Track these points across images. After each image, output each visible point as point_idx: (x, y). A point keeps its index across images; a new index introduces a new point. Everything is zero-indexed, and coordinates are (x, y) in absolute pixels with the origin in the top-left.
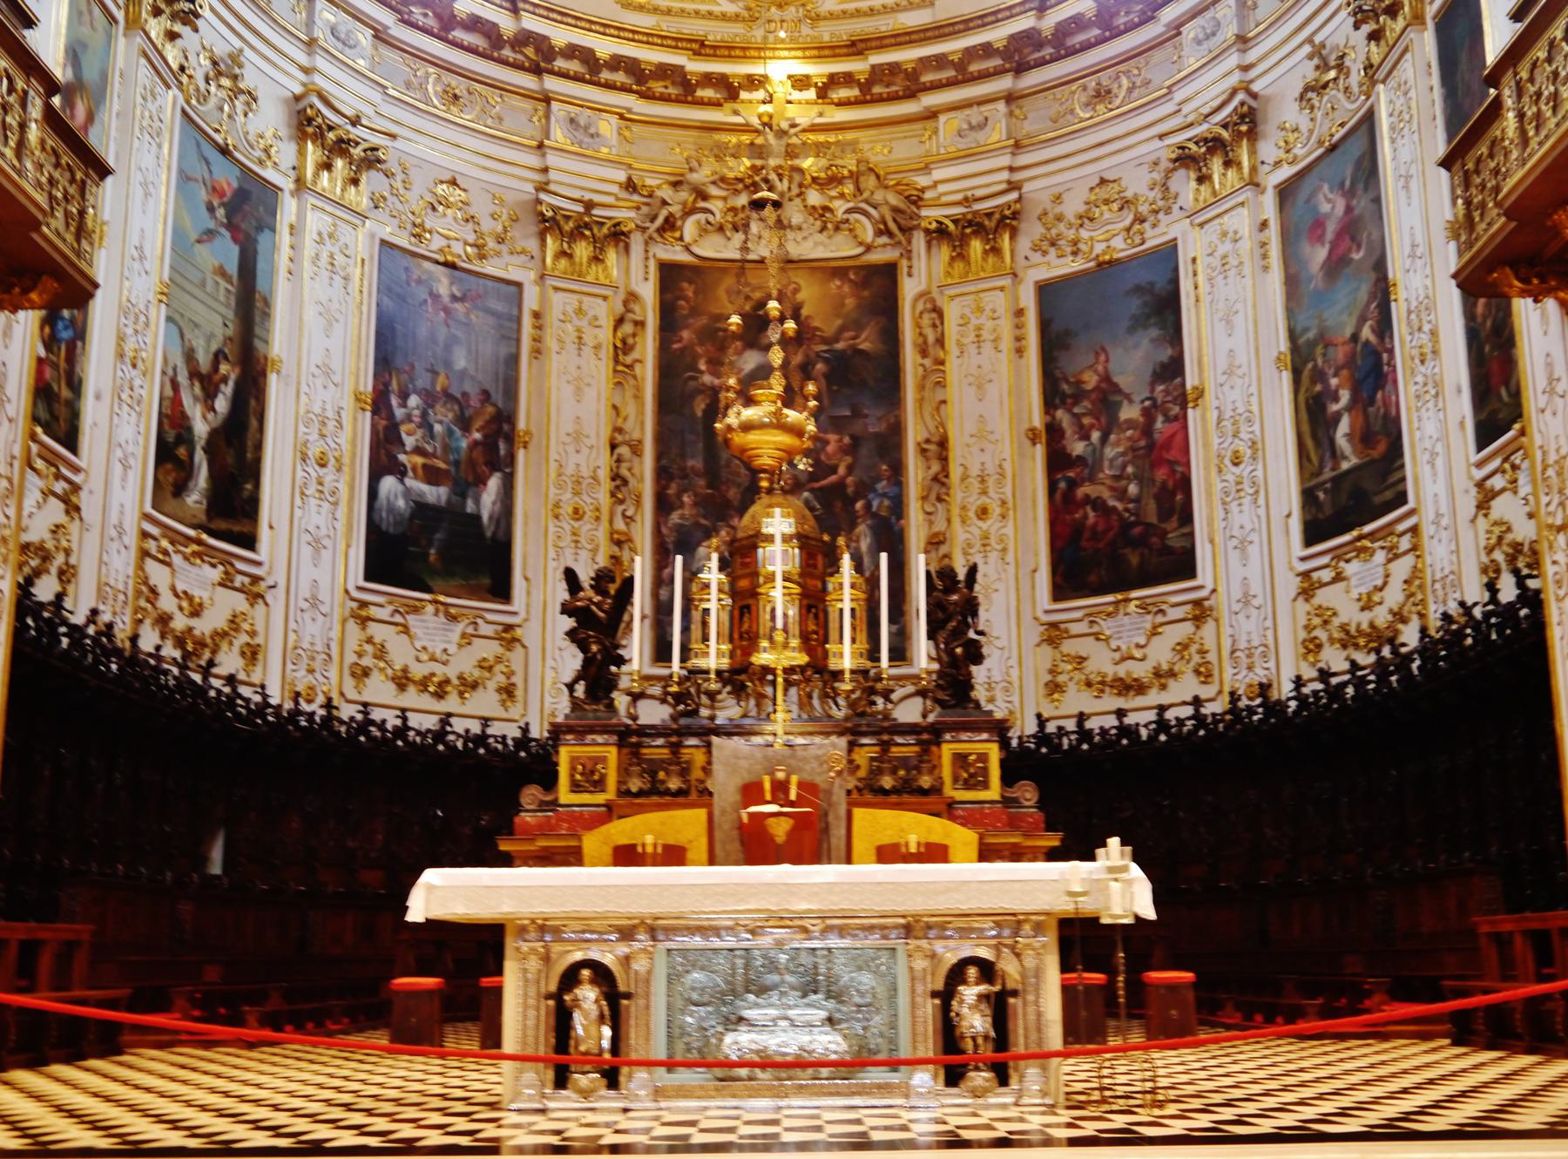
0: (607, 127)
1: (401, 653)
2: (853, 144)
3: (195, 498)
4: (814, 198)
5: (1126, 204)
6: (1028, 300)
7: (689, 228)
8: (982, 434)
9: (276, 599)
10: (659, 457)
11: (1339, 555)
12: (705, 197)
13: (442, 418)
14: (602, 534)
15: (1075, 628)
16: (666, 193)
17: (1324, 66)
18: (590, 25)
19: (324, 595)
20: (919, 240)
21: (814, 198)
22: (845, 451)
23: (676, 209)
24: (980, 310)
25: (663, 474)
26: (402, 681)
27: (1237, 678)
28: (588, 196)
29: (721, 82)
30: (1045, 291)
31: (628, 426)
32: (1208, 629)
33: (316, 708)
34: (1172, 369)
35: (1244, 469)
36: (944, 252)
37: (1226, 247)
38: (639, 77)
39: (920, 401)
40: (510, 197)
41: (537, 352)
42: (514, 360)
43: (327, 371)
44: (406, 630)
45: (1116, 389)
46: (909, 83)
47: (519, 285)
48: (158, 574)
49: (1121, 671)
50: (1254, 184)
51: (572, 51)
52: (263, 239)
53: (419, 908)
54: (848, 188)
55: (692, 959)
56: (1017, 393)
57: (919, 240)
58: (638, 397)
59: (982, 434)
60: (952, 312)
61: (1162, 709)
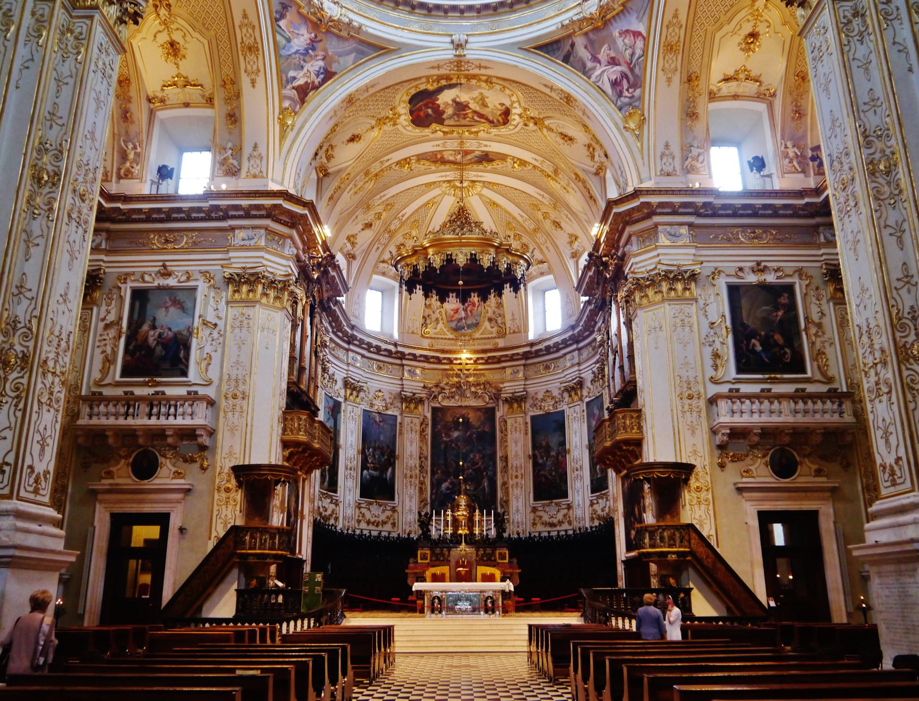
1: (368, 515)
2: (483, 375)
3: (326, 484)
4: (473, 389)
5: (553, 398)
6: (529, 420)
7: (440, 398)
8: (516, 456)
9: (341, 505)
10: (432, 460)
11: (598, 497)
12: (444, 389)
13: (378, 452)
14: (417, 482)
16: (433, 389)
17: (595, 377)
18: (415, 348)
20: (501, 403)
21: (473, 389)
22: (480, 458)
23: (436, 393)
24: (516, 422)
25: (432, 464)
26: (368, 523)
27: (576, 525)
29: (449, 359)
30: (532, 418)
31: (424, 452)
32: (571, 511)
34: (563, 443)
35: (579, 472)
36: (507, 406)
37: (575, 415)
39: (501, 446)
41: (401, 434)
42: (395, 436)
43: (351, 446)
44: (369, 509)
45: (550, 447)
46: (499, 360)
50: (581, 399)
51: (410, 354)
53: (414, 589)
54: (482, 387)
55: (450, 596)
56: (525, 445)
57: (501, 403)
58: (427, 444)
59: (516, 456)
61: (559, 532)
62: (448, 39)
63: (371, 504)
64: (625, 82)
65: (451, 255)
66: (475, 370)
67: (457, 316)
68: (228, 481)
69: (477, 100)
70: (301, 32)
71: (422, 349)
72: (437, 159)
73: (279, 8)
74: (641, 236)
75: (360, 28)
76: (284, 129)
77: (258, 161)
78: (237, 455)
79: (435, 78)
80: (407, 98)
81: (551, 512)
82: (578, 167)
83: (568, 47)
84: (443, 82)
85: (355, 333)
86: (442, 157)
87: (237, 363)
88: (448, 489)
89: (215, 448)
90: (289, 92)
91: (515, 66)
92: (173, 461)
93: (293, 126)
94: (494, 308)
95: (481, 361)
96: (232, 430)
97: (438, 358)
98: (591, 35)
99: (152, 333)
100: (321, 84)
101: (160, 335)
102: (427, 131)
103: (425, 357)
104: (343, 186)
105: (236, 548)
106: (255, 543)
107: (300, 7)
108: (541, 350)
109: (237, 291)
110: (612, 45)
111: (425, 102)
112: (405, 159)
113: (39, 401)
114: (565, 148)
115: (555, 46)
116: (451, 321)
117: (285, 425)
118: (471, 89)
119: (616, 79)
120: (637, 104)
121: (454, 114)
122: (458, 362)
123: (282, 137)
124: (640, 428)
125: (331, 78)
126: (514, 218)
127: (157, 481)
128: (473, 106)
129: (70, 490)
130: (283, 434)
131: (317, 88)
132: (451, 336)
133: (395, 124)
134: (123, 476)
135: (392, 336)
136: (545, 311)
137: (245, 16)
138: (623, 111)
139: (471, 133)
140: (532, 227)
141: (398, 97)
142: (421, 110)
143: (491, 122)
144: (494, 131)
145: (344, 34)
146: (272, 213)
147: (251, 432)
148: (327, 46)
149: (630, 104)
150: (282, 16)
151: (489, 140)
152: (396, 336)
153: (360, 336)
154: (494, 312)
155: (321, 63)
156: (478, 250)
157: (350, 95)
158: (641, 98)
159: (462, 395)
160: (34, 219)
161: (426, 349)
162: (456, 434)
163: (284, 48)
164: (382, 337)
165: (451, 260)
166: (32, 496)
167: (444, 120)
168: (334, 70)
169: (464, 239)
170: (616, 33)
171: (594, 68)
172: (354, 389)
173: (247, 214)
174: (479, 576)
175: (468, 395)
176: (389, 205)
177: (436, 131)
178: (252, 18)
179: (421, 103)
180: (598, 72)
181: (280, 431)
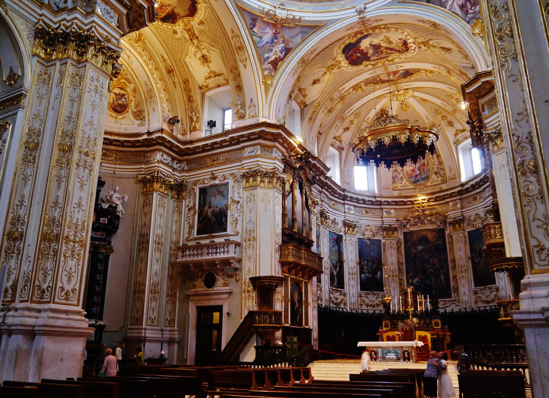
0: (392, 211)
1: (367, 301)
2: (435, 208)
4: (429, 218)
5: (481, 218)
6: (466, 234)
7: (408, 226)
8: (461, 258)
9: (348, 296)
13: (370, 263)
14: (397, 279)
15: (479, 292)
18: (387, 197)
19: (355, 294)
21: (429, 218)
24: (458, 236)
25: (407, 268)
26: (367, 305)
28: (391, 224)
29: (410, 201)
30: (469, 232)
31: (401, 260)
33: (354, 311)
38: (397, 203)
40: (378, 226)
41: (384, 250)
42: (381, 252)
44: (367, 297)
46: (443, 198)
47: (380, 240)
48: (332, 295)
49: (487, 299)
51: (385, 201)
52: (341, 244)
56: (465, 251)
58: (402, 255)
59: (461, 258)
60: (454, 237)
62: (354, 10)
63: (368, 294)
64: (468, 4)
65: (380, 139)
66: (428, 206)
67: (414, 174)
68: (249, 286)
69: (384, 40)
70: (267, 31)
71: (392, 197)
72: (376, 81)
73: (251, 21)
74: (490, 104)
75: (300, 19)
76: (267, 87)
77: (254, 108)
78: (252, 272)
79: (353, 35)
80: (340, 51)
81: (486, 294)
82: (459, 66)
84: (359, 36)
85: (346, 193)
86: (380, 79)
87: (250, 221)
88: (418, 282)
89: (242, 268)
90: (267, 66)
91: (397, 14)
92: (223, 277)
93: (272, 84)
94: (437, 166)
95: (432, 200)
96: (249, 258)
97: (403, 201)
99: (209, 210)
100: (284, 57)
101: (213, 210)
102: (361, 67)
103: (395, 202)
104: (317, 110)
105: (252, 324)
106: (261, 320)
107: (263, 18)
108: (468, 188)
109: (247, 182)
111: (353, 50)
112: (357, 84)
113: (64, 256)
114: (447, 55)
116: (411, 177)
117: (281, 253)
118: (377, 35)
120: (478, 16)
121: (374, 53)
122: (417, 202)
123: (267, 91)
124: (502, 235)
126: (439, 106)
127: (216, 288)
128: (383, 44)
129: (178, 295)
130: (280, 258)
132: (412, 187)
133: (339, 68)
134: (201, 288)
135: (374, 192)
136: (472, 162)
137: (233, 32)
138: (470, 23)
139: (389, 61)
140: (451, 109)
141: (335, 51)
142: (353, 56)
143: (399, 51)
144: (403, 56)
145: (292, 25)
146: (262, 135)
147: (259, 259)
148: (284, 34)
149: (474, 17)
150: (254, 26)
151: (403, 63)
152: (376, 192)
153: (349, 195)
154: (438, 168)
155: (282, 45)
156: (397, 132)
157: (302, 58)
158: (480, 12)
159: (423, 223)
160: (62, 169)
161: (395, 197)
162: (420, 248)
163: (259, 42)
164: (367, 194)
165: (381, 142)
166: (64, 301)
167: (369, 58)
168: (290, 47)
169: (387, 127)
172: (350, 226)
173: (249, 138)
174: (417, 337)
175: (426, 222)
176: (357, 114)
177: (367, 65)
178: (237, 32)
179: (351, 52)
181: (278, 257)
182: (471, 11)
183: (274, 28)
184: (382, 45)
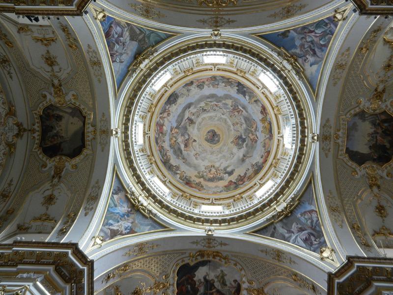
73: (116, 189)
83: (272, 230)
84: (200, 259)
98: (284, 221)
100: (125, 234)
107: (127, 192)
110: (298, 221)
115: (265, 230)
118: (215, 267)
119: (306, 238)
125: (133, 233)
131: (124, 235)
155: (130, 225)
168: (136, 230)
170: (299, 215)
171: (290, 237)
179: (184, 278)
180: (293, 237)
182: (316, 243)
183: (131, 207)
184: (215, 284)
